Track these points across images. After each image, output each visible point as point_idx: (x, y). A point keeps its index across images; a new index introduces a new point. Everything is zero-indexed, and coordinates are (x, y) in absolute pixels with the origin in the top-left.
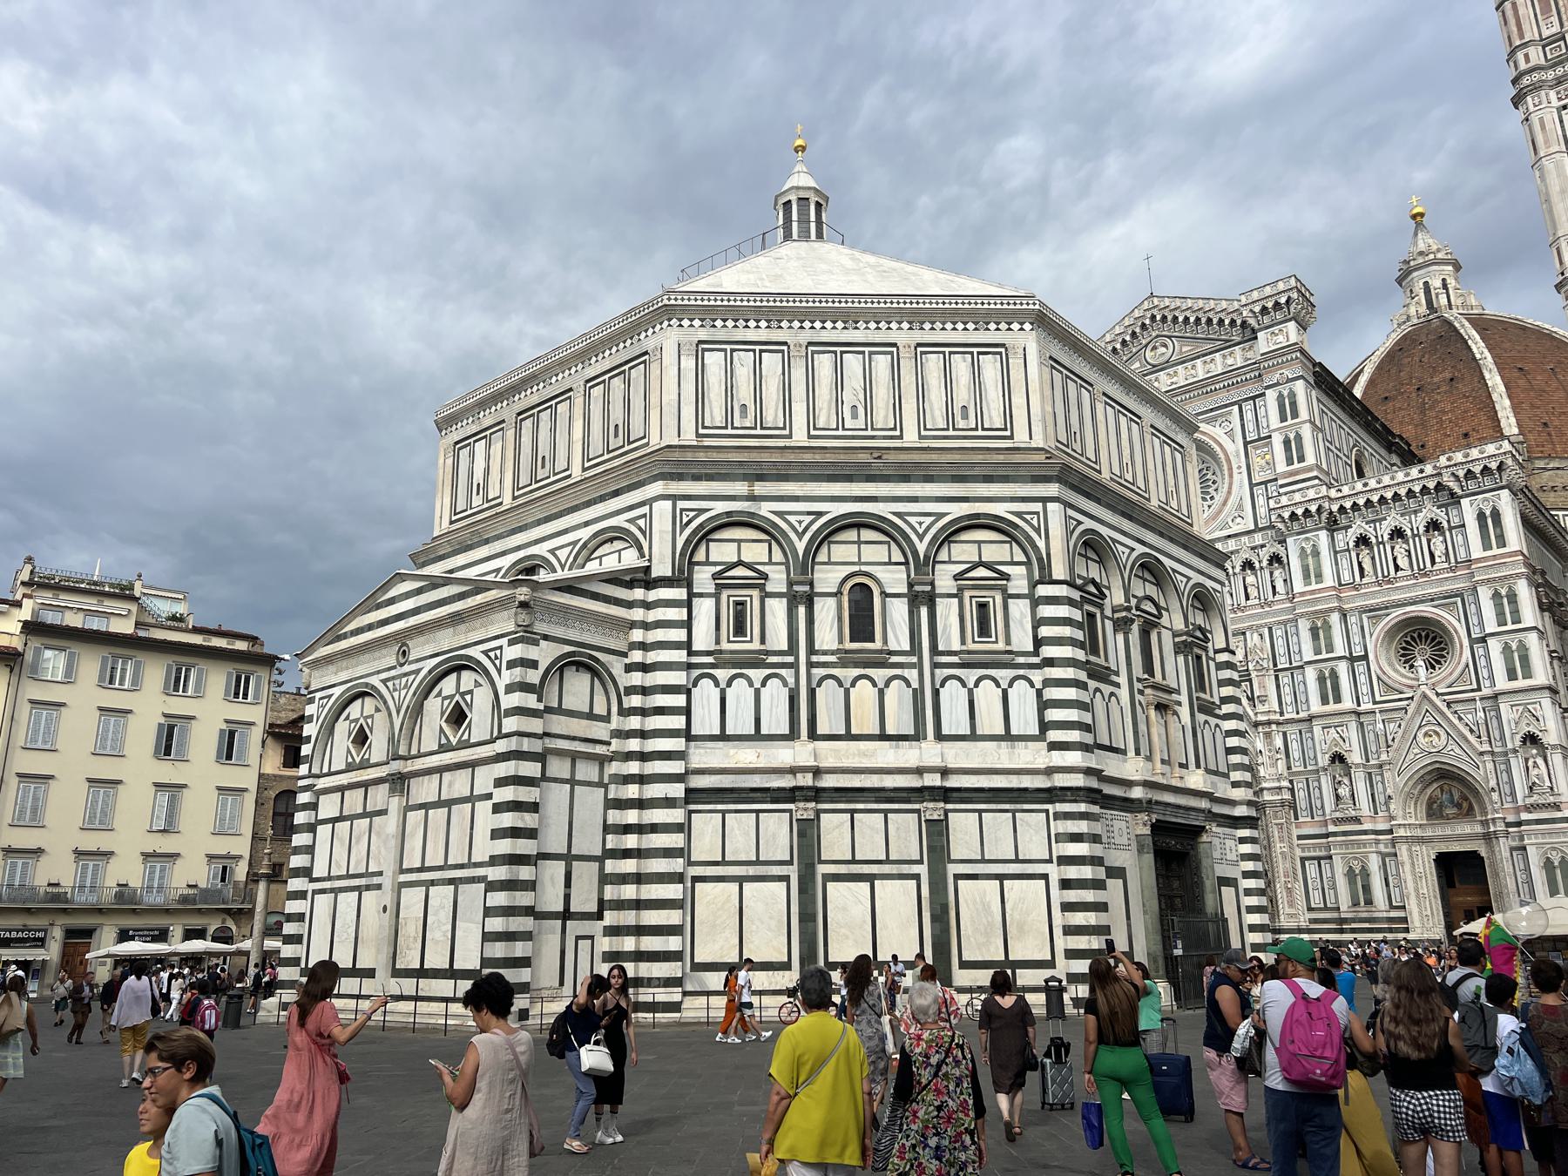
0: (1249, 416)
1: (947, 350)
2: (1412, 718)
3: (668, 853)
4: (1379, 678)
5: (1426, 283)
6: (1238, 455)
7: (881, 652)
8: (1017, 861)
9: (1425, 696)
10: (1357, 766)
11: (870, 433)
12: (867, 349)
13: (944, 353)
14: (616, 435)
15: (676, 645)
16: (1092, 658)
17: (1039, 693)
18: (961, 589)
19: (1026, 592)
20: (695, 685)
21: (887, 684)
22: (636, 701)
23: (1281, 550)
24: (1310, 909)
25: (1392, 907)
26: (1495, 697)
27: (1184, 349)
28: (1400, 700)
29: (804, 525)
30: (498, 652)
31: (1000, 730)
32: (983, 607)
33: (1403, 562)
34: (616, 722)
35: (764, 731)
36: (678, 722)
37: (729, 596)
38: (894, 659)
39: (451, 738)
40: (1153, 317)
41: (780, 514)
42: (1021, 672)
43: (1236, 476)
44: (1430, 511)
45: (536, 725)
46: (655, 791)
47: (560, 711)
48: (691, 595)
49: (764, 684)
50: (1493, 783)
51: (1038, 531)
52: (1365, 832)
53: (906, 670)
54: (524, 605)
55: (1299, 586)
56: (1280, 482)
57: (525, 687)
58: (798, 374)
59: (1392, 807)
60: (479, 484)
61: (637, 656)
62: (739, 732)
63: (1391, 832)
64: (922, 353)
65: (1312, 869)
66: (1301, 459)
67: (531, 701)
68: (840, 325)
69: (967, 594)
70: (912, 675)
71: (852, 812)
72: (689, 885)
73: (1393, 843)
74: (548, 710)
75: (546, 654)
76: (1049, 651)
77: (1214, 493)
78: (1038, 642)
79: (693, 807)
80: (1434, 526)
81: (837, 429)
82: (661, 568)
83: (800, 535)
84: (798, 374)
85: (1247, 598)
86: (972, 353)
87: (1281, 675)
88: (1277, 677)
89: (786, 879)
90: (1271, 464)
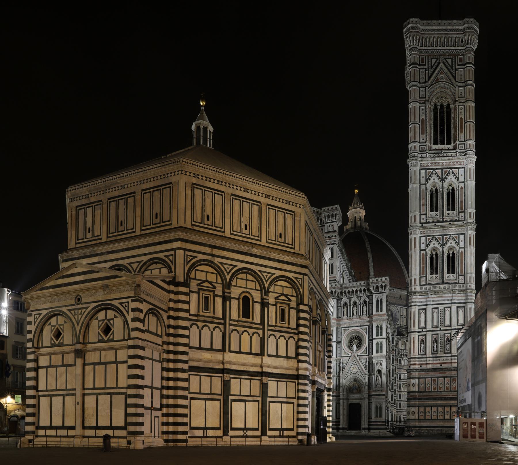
17: (297, 343)
18: (277, 303)
19: (295, 307)
21: (253, 335)
22: (172, 331)
31: (285, 355)
32: (283, 310)
34: (165, 338)
35: (214, 348)
36: (185, 341)
37: (203, 294)
39: (104, 337)
42: (292, 335)
46: (180, 366)
61: (172, 313)
69: (278, 305)
70: (260, 332)
71: (241, 379)
76: (302, 329)
78: (298, 325)
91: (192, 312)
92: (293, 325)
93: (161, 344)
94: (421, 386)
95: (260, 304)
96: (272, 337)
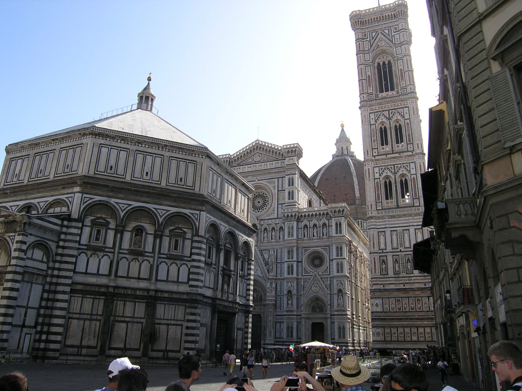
0: (280, 182)
1: (179, 160)
2: (311, 281)
3: (61, 309)
4: (304, 268)
5: (342, 147)
6: (275, 194)
7: (142, 251)
8: (174, 320)
9: (315, 275)
10: (295, 295)
11: (151, 181)
12: (154, 155)
13: (178, 160)
14: (67, 168)
15: (76, 242)
16: (207, 260)
17: (189, 269)
20: (79, 255)
21: (143, 262)
22: (58, 258)
23: (283, 225)
24: (276, 338)
25: (298, 338)
26: (333, 277)
27: (265, 158)
28: (309, 276)
29: (124, 208)
30: (13, 237)
31: (176, 280)
32: (177, 241)
33: (315, 234)
34: (51, 264)
35: (100, 272)
36: (71, 267)
38: (146, 254)
40: (257, 147)
41: (117, 203)
42: (185, 262)
43: (274, 200)
44: (324, 220)
45: (21, 263)
47: (31, 259)
48: (83, 225)
49: (102, 257)
50: (329, 303)
51: (197, 220)
52: (294, 315)
53: (150, 258)
54: (25, 223)
55: (286, 237)
56: (286, 205)
57: (20, 250)
58: (131, 159)
59: (302, 308)
60: (17, 174)
62: (92, 272)
63: (301, 315)
64: (171, 159)
65: (278, 325)
66: (293, 199)
67: (22, 255)
68: (147, 146)
72: (67, 319)
73: (301, 318)
74: (28, 258)
75: (30, 239)
76: (195, 257)
77: (267, 205)
78: (191, 254)
79: (72, 295)
80: (324, 224)
81: (141, 178)
82: (75, 215)
83: (123, 211)
84: (131, 159)
85: (272, 239)
86: (186, 162)
87: (278, 264)
88: (277, 265)
89: (100, 320)
90: (284, 198)
91: (83, 242)
92: (187, 253)
93: (46, 269)
94: (386, 306)
95: (153, 236)
96: (163, 264)
